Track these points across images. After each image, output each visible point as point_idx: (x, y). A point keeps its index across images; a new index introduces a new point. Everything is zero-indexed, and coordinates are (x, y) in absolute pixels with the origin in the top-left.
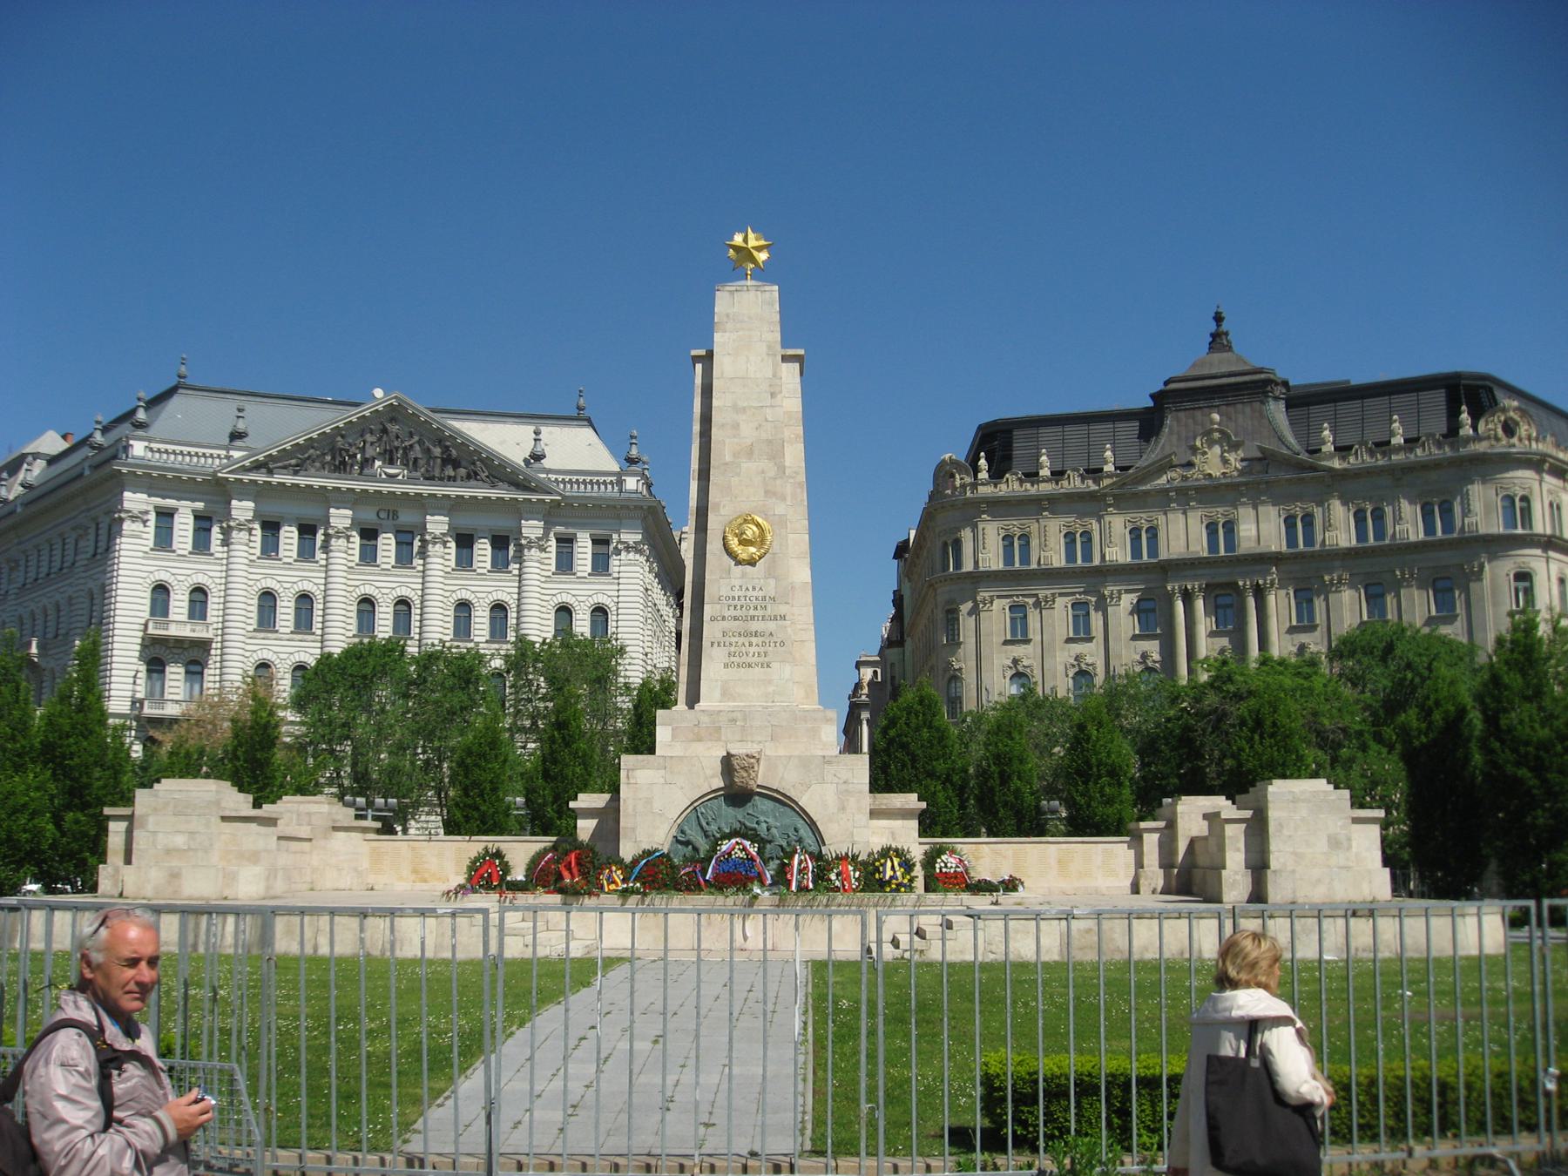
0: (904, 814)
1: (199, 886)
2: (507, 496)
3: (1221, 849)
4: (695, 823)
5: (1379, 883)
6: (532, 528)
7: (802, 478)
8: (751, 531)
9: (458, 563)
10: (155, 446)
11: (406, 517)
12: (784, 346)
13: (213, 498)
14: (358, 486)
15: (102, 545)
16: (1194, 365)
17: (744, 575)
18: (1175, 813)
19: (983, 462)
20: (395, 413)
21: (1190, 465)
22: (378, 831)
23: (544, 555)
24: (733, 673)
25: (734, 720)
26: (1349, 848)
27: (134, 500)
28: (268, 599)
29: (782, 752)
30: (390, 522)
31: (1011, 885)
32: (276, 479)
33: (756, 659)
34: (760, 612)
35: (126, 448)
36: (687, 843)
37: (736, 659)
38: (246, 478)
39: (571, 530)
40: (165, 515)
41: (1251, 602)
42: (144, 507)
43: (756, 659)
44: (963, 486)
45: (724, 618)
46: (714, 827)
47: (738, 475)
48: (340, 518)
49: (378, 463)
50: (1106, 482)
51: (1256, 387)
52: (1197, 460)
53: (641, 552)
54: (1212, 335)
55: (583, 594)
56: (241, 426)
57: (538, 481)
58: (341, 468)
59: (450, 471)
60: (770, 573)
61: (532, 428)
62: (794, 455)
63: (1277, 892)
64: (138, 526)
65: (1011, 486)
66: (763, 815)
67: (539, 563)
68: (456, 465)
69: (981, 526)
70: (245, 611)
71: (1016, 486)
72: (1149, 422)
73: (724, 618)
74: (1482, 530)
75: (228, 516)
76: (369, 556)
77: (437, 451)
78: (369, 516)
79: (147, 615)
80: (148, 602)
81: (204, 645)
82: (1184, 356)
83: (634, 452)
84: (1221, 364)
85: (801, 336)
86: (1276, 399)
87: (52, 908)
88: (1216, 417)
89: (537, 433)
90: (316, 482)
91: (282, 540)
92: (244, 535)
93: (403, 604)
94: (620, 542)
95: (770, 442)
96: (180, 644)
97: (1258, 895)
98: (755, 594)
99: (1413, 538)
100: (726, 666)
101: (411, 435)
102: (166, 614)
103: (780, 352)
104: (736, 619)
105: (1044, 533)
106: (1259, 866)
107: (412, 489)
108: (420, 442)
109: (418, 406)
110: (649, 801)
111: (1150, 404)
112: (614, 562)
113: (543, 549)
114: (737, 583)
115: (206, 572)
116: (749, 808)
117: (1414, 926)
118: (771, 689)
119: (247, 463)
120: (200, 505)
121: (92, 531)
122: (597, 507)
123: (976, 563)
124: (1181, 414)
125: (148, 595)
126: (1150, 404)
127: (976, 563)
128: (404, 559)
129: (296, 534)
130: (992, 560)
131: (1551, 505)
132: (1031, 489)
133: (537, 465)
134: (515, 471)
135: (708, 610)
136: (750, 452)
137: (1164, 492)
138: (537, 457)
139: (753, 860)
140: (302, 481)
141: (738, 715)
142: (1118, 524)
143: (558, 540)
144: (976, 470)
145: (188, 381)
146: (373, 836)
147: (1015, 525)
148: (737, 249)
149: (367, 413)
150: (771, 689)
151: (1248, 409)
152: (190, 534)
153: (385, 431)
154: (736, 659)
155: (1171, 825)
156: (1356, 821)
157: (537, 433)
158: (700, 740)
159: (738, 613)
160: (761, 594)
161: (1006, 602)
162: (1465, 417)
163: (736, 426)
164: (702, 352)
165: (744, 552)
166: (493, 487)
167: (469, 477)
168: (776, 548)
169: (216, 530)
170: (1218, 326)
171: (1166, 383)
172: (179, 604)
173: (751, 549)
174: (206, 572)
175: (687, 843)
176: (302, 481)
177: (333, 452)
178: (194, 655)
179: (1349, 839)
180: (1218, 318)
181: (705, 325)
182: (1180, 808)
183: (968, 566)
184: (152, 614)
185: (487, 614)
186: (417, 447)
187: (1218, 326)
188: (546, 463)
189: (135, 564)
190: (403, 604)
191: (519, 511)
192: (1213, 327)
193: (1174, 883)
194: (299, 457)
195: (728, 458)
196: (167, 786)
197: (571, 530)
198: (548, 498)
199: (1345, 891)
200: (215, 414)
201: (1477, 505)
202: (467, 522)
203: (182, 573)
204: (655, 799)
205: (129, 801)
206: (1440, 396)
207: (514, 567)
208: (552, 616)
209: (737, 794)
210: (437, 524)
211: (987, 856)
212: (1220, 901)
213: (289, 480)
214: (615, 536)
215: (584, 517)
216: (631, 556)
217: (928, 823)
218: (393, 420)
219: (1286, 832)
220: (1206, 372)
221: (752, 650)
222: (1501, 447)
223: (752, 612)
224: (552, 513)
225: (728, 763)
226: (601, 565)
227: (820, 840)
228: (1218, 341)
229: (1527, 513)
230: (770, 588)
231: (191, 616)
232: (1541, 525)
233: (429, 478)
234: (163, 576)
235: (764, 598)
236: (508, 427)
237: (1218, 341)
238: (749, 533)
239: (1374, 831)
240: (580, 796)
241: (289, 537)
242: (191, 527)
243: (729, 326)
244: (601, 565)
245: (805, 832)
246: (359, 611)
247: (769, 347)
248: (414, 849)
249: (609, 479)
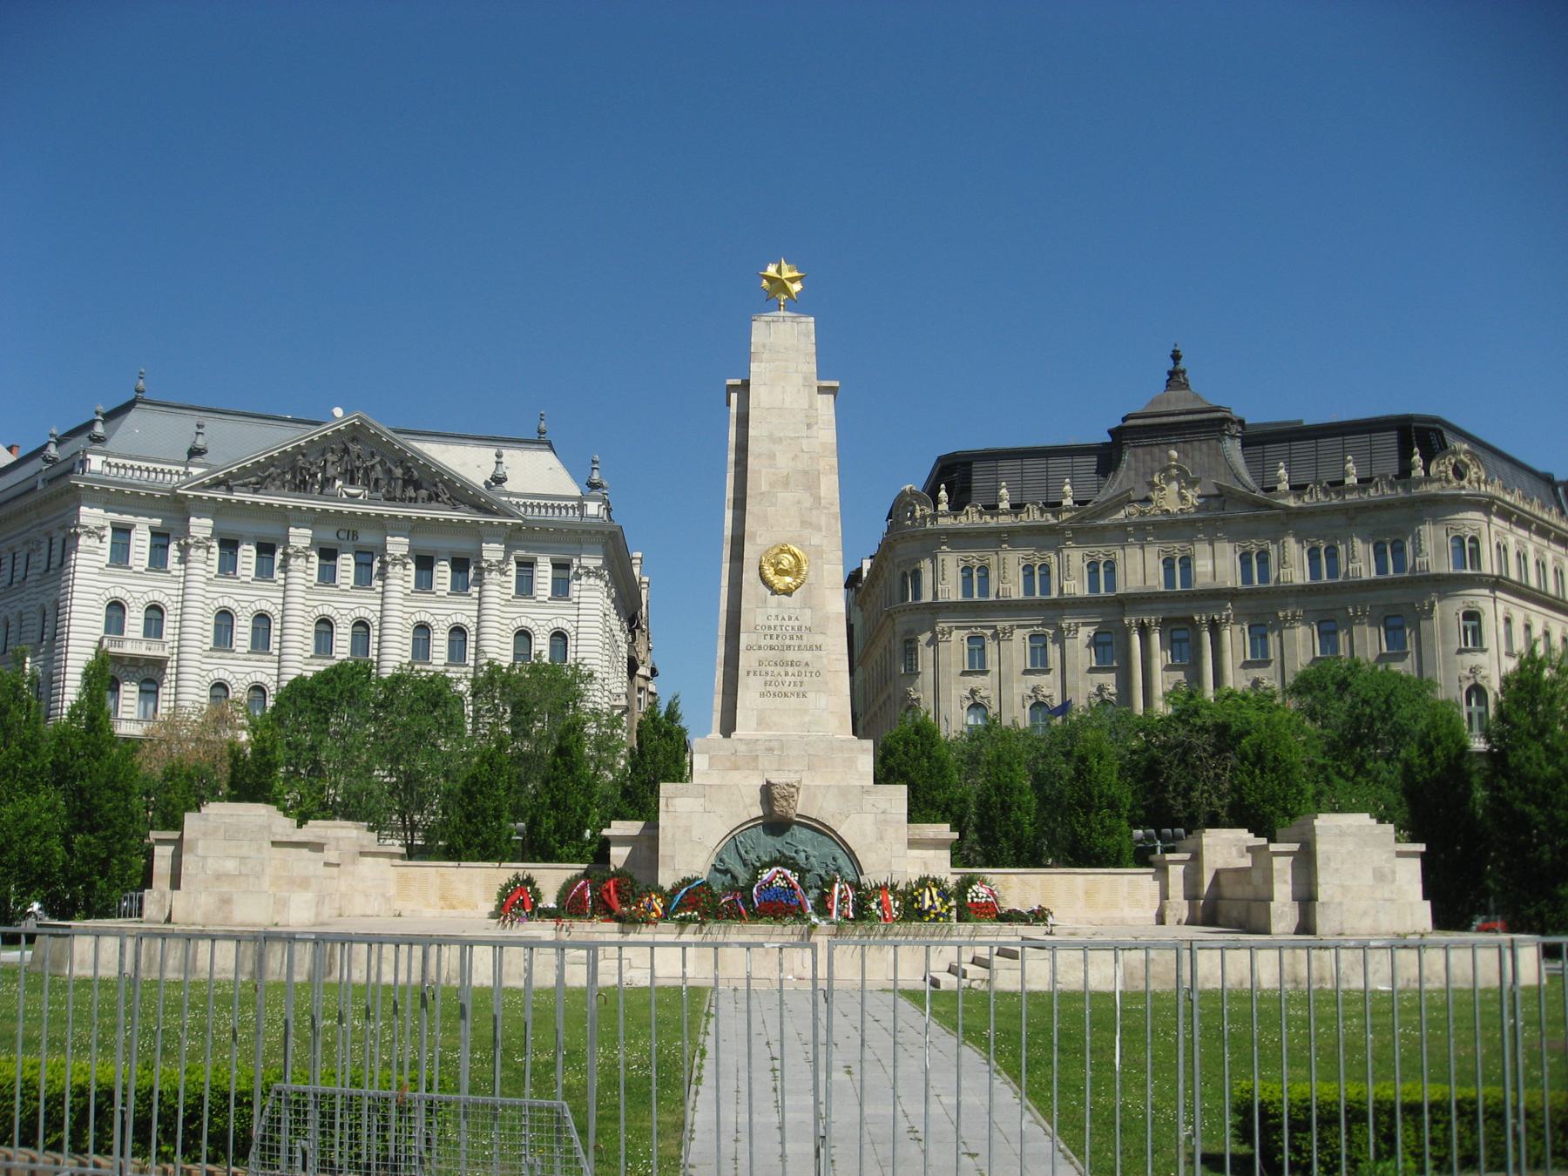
0: (936, 844)
1: (252, 913)
2: (469, 519)
3: (1269, 881)
4: (733, 853)
5: (1421, 914)
6: (492, 552)
7: (836, 509)
8: (787, 561)
9: (518, 590)
10: (113, 461)
11: (367, 538)
12: (819, 378)
13: (172, 512)
14: (319, 505)
15: (56, 560)
16: (1152, 403)
17: (779, 605)
18: (1200, 846)
19: (943, 494)
20: (356, 432)
21: (1148, 500)
22: (402, 857)
23: (504, 578)
24: (769, 702)
25: (771, 750)
26: (1394, 881)
27: (90, 515)
28: (225, 618)
29: (818, 782)
30: (350, 543)
31: (1040, 916)
32: (236, 497)
33: (792, 688)
34: (795, 642)
35: (83, 462)
36: (726, 872)
37: (772, 689)
38: (206, 495)
39: (531, 554)
40: (122, 532)
41: (1207, 637)
42: (100, 523)
43: (792, 688)
44: (924, 517)
45: (760, 648)
47: (774, 505)
48: (300, 537)
49: (339, 483)
50: (1065, 516)
51: (1212, 425)
52: (1155, 495)
53: (601, 577)
55: (542, 618)
56: (200, 442)
57: (500, 504)
58: (301, 487)
59: (411, 492)
60: (806, 603)
61: (494, 451)
62: (829, 486)
63: (1325, 923)
64: (94, 542)
65: (971, 518)
66: (802, 844)
67: (501, 586)
68: (418, 486)
69: (940, 557)
70: (201, 629)
71: (976, 518)
72: (1107, 458)
73: (760, 648)
74: (1433, 570)
75: (187, 534)
76: (327, 576)
77: (399, 472)
78: (329, 536)
79: (101, 632)
80: (102, 618)
81: (159, 664)
83: (596, 477)
84: (1178, 402)
85: (837, 367)
86: (1233, 437)
87: (98, 934)
88: (1174, 454)
89: (499, 456)
90: (276, 501)
91: (240, 559)
92: (202, 553)
93: (362, 625)
94: (580, 566)
95: (805, 473)
96: (135, 661)
97: (1306, 926)
98: (791, 623)
99: (1365, 577)
100: (762, 695)
101: (373, 455)
102: (121, 631)
103: (816, 383)
104: (772, 648)
105: (1002, 565)
106: (1306, 899)
107: (373, 510)
108: (382, 463)
109: (381, 426)
110: (688, 829)
111: (1109, 439)
112: (574, 586)
113: (504, 573)
114: (773, 612)
115: (162, 590)
116: (787, 837)
117: (1460, 958)
118: (807, 719)
119: (206, 480)
120: (157, 522)
121: (45, 546)
122: (559, 531)
123: (935, 594)
124: (1139, 451)
125: (103, 612)
126: (1109, 439)
127: (935, 594)
128: (363, 580)
129: (254, 553)
130: (952, 591)
131: (1498, 546)
132: (990, 521)
133: (498, 488)
134: (477, 494)
135: (744, 639)
136: (786, 483)
137: (1122, 527)
138: (499, 480)
139: (793, 888)
140: (262, 499)
141: (775, 744)
142: (1076, 557)
143: (519, 564)
144: (936, 502)
145: (146, 396)
146: (398, 862)
147: (974, 558)
148: (770, 279)
149: (329, 432)
150: (807, 719)
151: (1204, 447)
152: (147, 550)
153: (346, 450)
154: (772, 689)
155: (1197, 856)
156: (1400, 854)
157: (499, 456)
158: (737, 769)
159: (774, 642)
160: (797, 623)
161: (964, 633)
162: (1417, 458)
163: (772, 456)
164: (739, 382)
165: (782, 582)
166: (455, 509)
167: (430, 499)
168: (811, 579)
169: (173, 547)
171: (1124, 419)
172: (135, 621)
173: (786, 579)
174: (162, 590)
175: (726, 872)
176: (262, 499)
177: (294, 471)
178: (150, 674)
179: (1394, 872)
180: (1176, 357)
181: (742, 355)
182: (1206, 840)
183: (927, 597)
184: (107, 631)
185: (446, 636)
186: (378, 467)
188: (507, 486)
189: (91, 580)
190: (362, 625)
191: (480, 534)
192: (1170, 365)
193: (1199, 914)
194: (259, 475)
195: (764, 488)
196: (218, 812)
197: (531, 554)
198: (509, 521)
199: (1391, 923)
200: (176, 430)
201: (1428, 545)
202: (428, 543)
203: (138, 590)
204: (695, 827)
205: (178, 825)
206: (1392, 438)
207: (474, 590)
208: (511, 640)
209: (775, 823)
210: (398, 546)
211: (1015, 887)
212: (1266, 931)
213: (249, 498)
214: (576, 561)
215: (544, 541)
216: (592, 580)
217: (960, 856)
218: (354, 440)
219: (1333, 865)
220: (1163, 409)
221: (788, 679)
222: (1453, 488)
223: (788, 642)
224: (513, 537)
225: (767, 792)
226: (561, 590)
227: (859, 870)
228: (1175, 378)
229: (1476, 553)
230: (807, 618)
231: (147, 633)
232: (1489, 566)
233: (390, 499)
234: (119, 593)
235: (800, 628)
236: (527, 454)
237: (1175, 378)
238: (785, 562)
239: (1415, 865)
241: (247, 555)
242: (148, 544)
243: (766, 356)
244: (561, 590)
245: (843, 861)
246: (317, 632)
247: (805, 379)
248: (442, 875)
249: (570, 504)
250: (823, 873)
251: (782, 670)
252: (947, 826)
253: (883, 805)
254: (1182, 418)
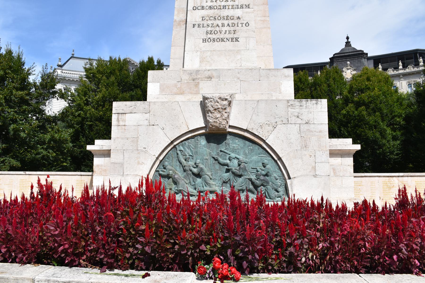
0: (341, 154)
16: (342, 50)
45: (203, 8)
46: (191, 163)
54: (346, 43)
82: (338, 47)
84: (349, 50)
86: (365, 58)
88: (349, 63)
100: (204, 41)
110: (136, 140)
118: (239, 57)
124: (339, 63)
141: (215, 74)
151: (357, 61)
170: (348, 40)
171: (334, 55)
180: (348, 38)
187: (348, 40)
192: (346, 41)
228: (348, 44)
237: (348, 44)
240: (97, 142)
245: (271, 166)
250: (253, 177)
251: (220, 23)
252: (350, 140)
253: (305, 118)
254: (350, 54)
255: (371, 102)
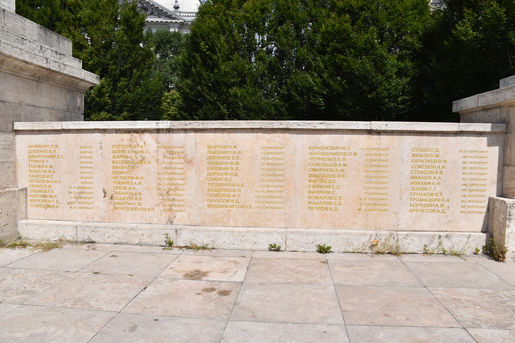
2: (164, 21)
166: (159, 17)
167: (151, 14)
198: (179, 21)
255: (362, 9)
